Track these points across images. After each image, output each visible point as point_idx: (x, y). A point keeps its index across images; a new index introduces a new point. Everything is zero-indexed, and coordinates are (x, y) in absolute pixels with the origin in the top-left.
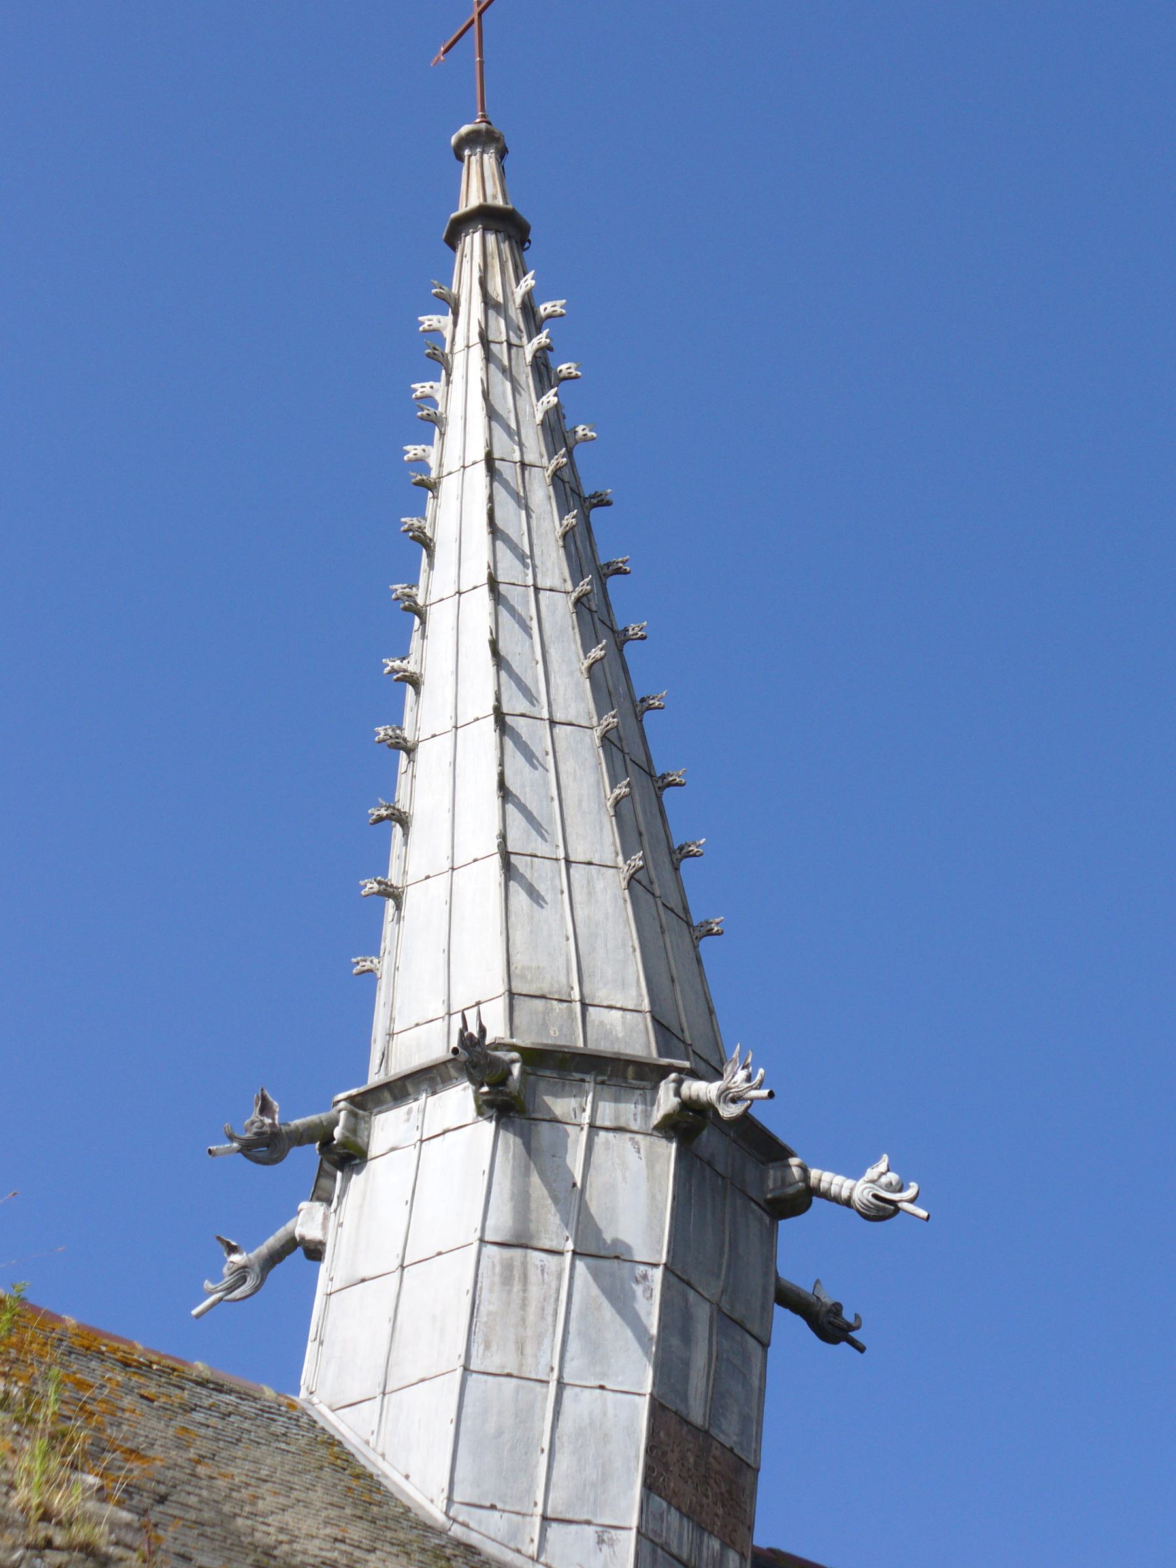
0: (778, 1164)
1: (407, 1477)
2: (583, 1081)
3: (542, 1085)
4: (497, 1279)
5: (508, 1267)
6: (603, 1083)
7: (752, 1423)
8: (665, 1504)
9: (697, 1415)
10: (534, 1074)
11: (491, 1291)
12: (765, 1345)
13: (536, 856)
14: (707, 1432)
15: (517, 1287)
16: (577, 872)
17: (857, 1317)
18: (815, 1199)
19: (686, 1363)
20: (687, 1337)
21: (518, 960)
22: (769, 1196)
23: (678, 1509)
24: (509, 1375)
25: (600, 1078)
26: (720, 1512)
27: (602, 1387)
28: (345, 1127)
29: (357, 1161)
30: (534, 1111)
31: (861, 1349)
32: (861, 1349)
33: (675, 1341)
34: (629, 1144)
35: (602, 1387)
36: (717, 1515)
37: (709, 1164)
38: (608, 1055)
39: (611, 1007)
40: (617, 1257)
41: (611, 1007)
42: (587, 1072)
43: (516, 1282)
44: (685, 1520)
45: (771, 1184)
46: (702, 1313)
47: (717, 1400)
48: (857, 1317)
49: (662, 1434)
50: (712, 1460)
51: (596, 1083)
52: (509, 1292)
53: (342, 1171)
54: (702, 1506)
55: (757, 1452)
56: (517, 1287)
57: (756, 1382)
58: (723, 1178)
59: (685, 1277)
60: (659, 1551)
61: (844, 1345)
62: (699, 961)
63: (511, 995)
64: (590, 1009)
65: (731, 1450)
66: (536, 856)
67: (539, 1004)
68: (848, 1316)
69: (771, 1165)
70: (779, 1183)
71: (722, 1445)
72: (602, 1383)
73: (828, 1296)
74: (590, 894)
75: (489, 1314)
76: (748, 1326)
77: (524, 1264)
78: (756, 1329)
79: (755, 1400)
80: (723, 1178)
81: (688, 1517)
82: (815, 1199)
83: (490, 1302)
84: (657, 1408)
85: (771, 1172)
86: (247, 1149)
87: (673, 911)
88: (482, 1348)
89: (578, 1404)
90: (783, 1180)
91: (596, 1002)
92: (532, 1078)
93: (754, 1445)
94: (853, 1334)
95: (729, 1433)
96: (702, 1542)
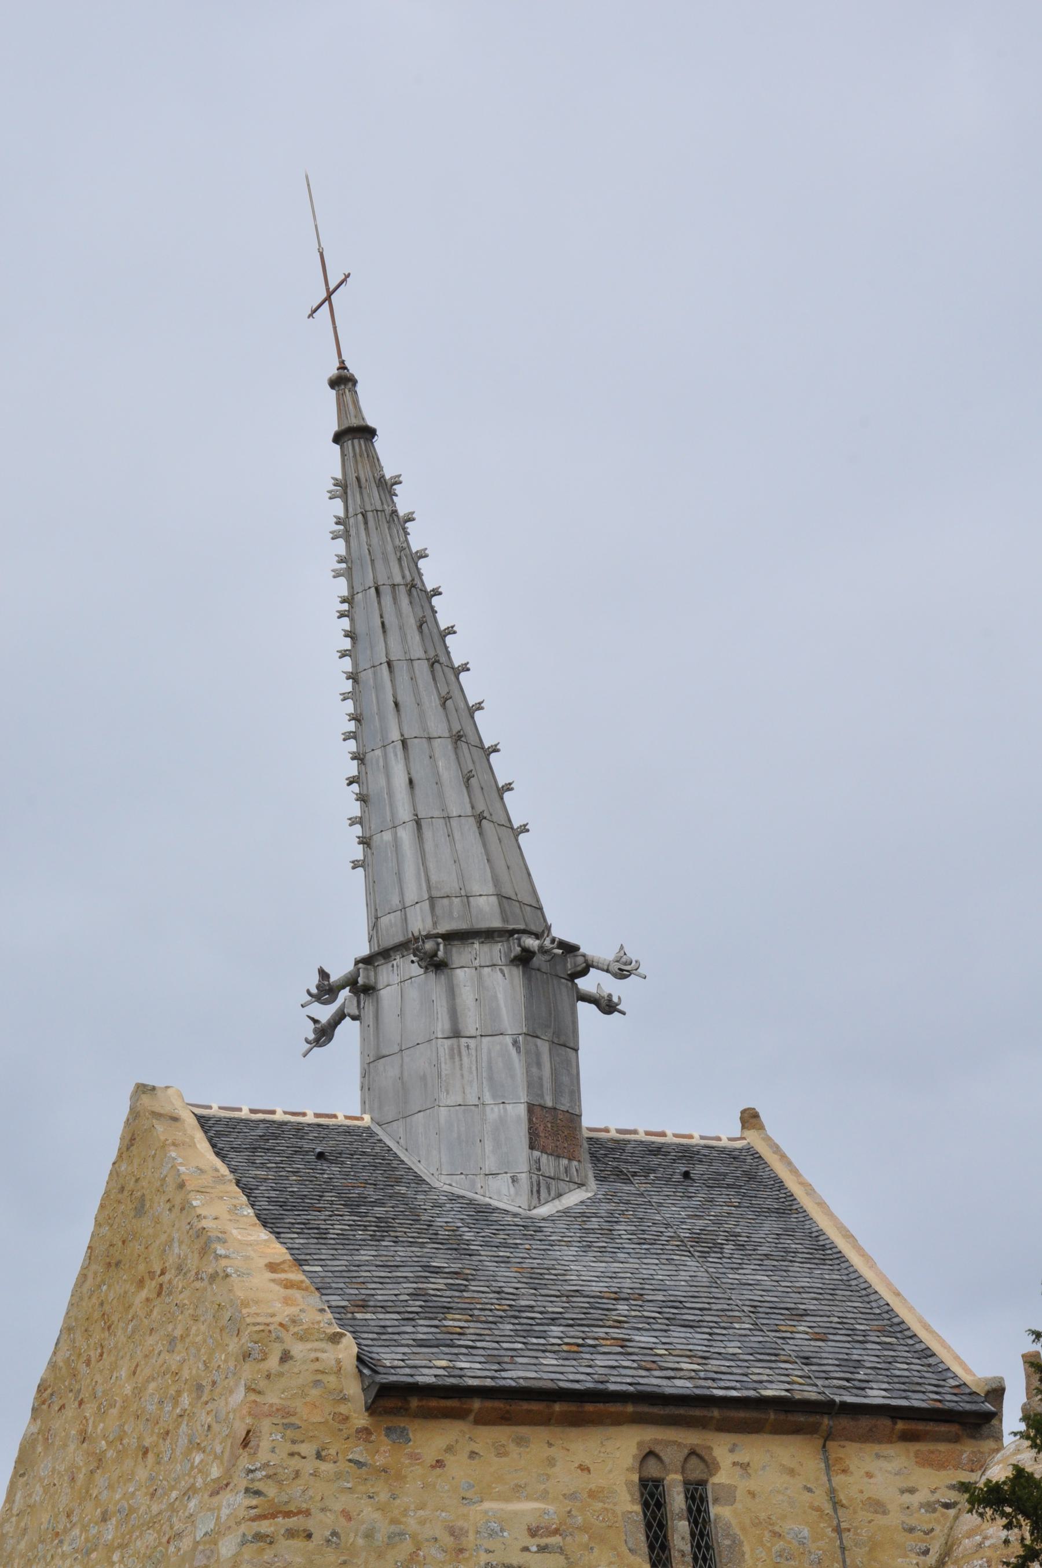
0: (572, 955)
1: (419, 1161)
2: (473, 943)
3: (454, 950)
4: (447, 1057)
5: (452, 1049)
6: (482, 943)
7: (575, 1094)
8: (540, 1153)
9: (549, 1104)
10: (450, 944)
11: (446, 1063)
12: (576, 1050)
13: (433, 818)
14: (555, 1109)
15: (457, 1059)
16: (454, 823)
17: (619, 998)
18: (591, 969)
19: (541, 1078)
20: (539, 1065)
21: (434, 878)
22: (569, 972)
23: (546, 1153)
24: (460, 1105)
25: (481, 940)
26: (566, 1145)
27: (503, 1103)
28: (364, 977)
29: (371, 991)
30: (452, 964)
31: (624, 1013)
32: (624, 1013)
33: (534, 1070)
34: (499, 973)
35: (503, 1103)
36: (565, 1148)
37: (539, 970)
38: (483, 930)
39: (481, 895)
40: (502, 1034)
41: (481, 895)
42: (474, 938)
43: (456, 1056)
44: (550, 1157)
45: (569, 967)
47: (557, 1091)
48: (619, 998)
49: (534, 1119)
50: (559, 1121)
51: (480, 943)
52: (454, 1062)
53: (364, 994)
54: (557, 1147)
55: (580, 1106)
56: (457, 1059)
57: (574, 1072)
58: (546, 973)
59: (535, 1035)
60: (541, 1177)
61: (616, 1013)
62: (520, 848)
63: (432, 900)
64: (471, 898)
65: (568, 1112)
66: (433, 818)
67: (446, 901)
68: (615, 999)
69: (568, 956)
70: (573, 965)
71: (563, 1111)
72: (503, 1101)
74: (462, 833)
75: (446, 1075)
76: (568, 1045)
77: (459, 1046)
78: (572, 1045)
79: (576, 1084)
80: (546, 973)
81: (551, 1155)
82: (591, 969)
83: (446, 1070)
84: (531, 1109)
85: (569, 960)
87: (503, 825)
88: (445, 1094)
90: (575, 964)
91: (474, 894)
92: (449, 946)
93: (577, 1104)
94: (618, 1007)
95: (565, 1105)
96: (559, 1163)
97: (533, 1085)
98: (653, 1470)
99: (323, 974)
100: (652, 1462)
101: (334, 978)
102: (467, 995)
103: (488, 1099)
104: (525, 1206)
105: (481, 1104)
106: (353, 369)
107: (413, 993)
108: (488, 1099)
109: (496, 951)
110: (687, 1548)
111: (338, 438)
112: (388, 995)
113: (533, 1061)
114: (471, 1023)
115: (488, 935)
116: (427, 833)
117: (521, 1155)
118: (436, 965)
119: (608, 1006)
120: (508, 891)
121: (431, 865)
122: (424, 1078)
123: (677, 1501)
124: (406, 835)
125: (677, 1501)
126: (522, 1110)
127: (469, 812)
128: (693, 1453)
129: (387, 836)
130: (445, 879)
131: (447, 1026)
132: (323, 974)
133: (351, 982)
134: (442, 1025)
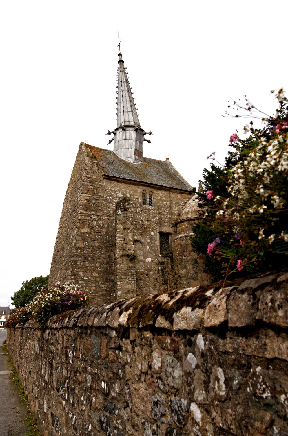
7: (142, 150)
9: (138, 150)
20: (137, 144)
46: (138, 143)
47: (139, 148)
73: (149, 140)
84: (135, 150)
86: (108, 134)
89: (130, 150)
95: (140, 150)
97: (136, 147)
98: (145, 192)
99: (109, 131)
100: (144, 191)
101: (110, 132)
102: (128, 134)
103: (129, 147)
104: (133, 161)
105: (128, 148)
106: (121, 53)
107: (121, 133)
108: (129, 147)
109: (133, 129)
110: (148, 202)
111: (119, 62)
112: (118, 135)
113: (136, 144)
114: (128, 138)
115: (131, 126)
116: (125, 113)
117: (133, 156)
118: (124, 130)
119: (149, 142)
120: (135, 122)
121: (125, 117)
122: (121, 145)
123: (148, 196)
124: (122, 114)
125: (148, 196)
126: (134, 150)
127: (131, 111)
128: (151, 191)
129: (120, 114)
130: (127, 119)
131: (125, 138)
132: (109, 131)
133: (113, 132)
134: (124, 137)
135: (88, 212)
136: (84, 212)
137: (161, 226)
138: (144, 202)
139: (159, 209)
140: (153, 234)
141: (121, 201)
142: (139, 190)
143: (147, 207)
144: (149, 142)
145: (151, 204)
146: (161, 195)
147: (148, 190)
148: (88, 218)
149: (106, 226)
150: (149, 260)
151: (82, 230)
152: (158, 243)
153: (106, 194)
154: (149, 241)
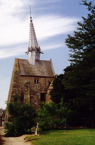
97: (36, 58)
113: (36, 57)
119: (43, 53)
123: (37, 81)
125: (37, 81)
135: (15, 89)
136: (14, 89)
137: (41, 91)
138: (35, 83)
139: (41, 85)
140: (38, 94)
141: (26, 84)
142: (33, 78)
143: (36, 84)
144: (43, 53)
145: (38, 83)
146: (42, 79)
147: (37, 78)
148: (15, 90)
149: (21, 92)
150: (36, 103)
151: (13, 95)
152: (40, 97)
153: (21, 81)
154: (36, 97)
